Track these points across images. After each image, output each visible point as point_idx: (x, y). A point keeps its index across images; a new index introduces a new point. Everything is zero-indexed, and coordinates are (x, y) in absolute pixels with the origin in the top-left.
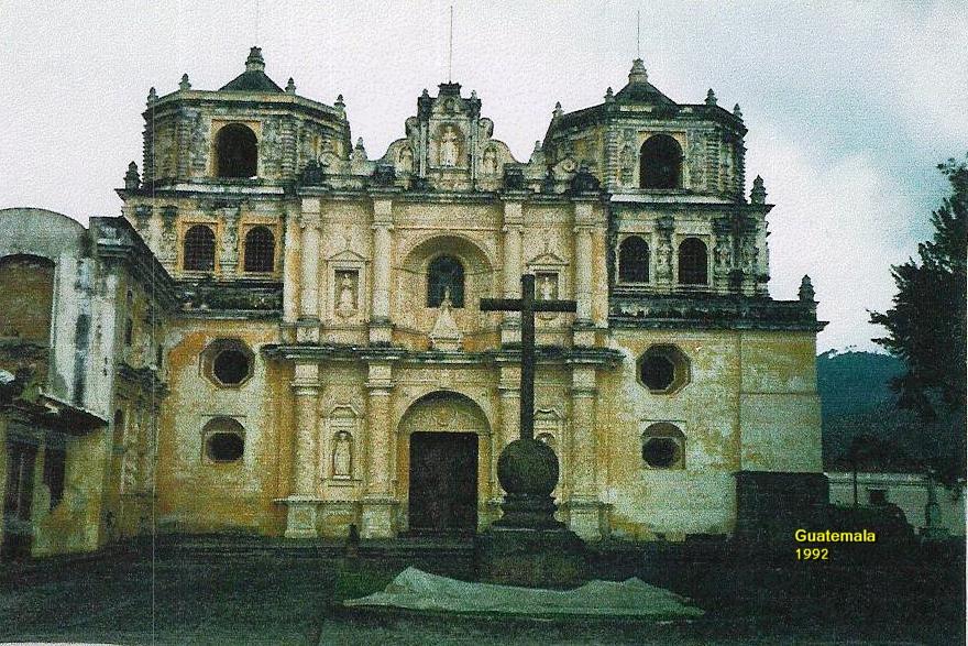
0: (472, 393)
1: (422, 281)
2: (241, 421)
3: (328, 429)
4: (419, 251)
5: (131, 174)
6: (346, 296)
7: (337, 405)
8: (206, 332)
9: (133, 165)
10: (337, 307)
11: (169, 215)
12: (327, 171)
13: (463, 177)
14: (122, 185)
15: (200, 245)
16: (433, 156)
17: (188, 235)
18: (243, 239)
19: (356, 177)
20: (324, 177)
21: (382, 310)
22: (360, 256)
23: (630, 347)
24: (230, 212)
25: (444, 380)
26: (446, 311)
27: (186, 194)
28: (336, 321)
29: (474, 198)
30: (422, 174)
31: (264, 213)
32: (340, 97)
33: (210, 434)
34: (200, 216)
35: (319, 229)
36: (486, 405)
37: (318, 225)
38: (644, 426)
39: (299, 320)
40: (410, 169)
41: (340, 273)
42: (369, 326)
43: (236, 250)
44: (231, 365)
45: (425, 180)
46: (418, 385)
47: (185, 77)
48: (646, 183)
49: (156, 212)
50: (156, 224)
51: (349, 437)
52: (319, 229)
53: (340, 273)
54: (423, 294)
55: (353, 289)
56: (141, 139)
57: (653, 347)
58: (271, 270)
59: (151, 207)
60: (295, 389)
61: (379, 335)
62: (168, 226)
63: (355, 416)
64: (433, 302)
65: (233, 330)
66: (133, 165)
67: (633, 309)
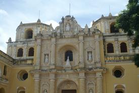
0: (73, 79)
2: (25, 88)
4: (61, 49)
6: (47, 59)
9: (10, 38)
16: (64, 29)
23: (111, 66)
25: (67, 77)
29: (74, 37)
36: (77, 83)
38: (115, 86)
41: (45, 55)
48: (111, 32)
53: (45, 55)
54: (64, 58)
57: (116, 67)
66: (10, 38)
67: (111, 58)
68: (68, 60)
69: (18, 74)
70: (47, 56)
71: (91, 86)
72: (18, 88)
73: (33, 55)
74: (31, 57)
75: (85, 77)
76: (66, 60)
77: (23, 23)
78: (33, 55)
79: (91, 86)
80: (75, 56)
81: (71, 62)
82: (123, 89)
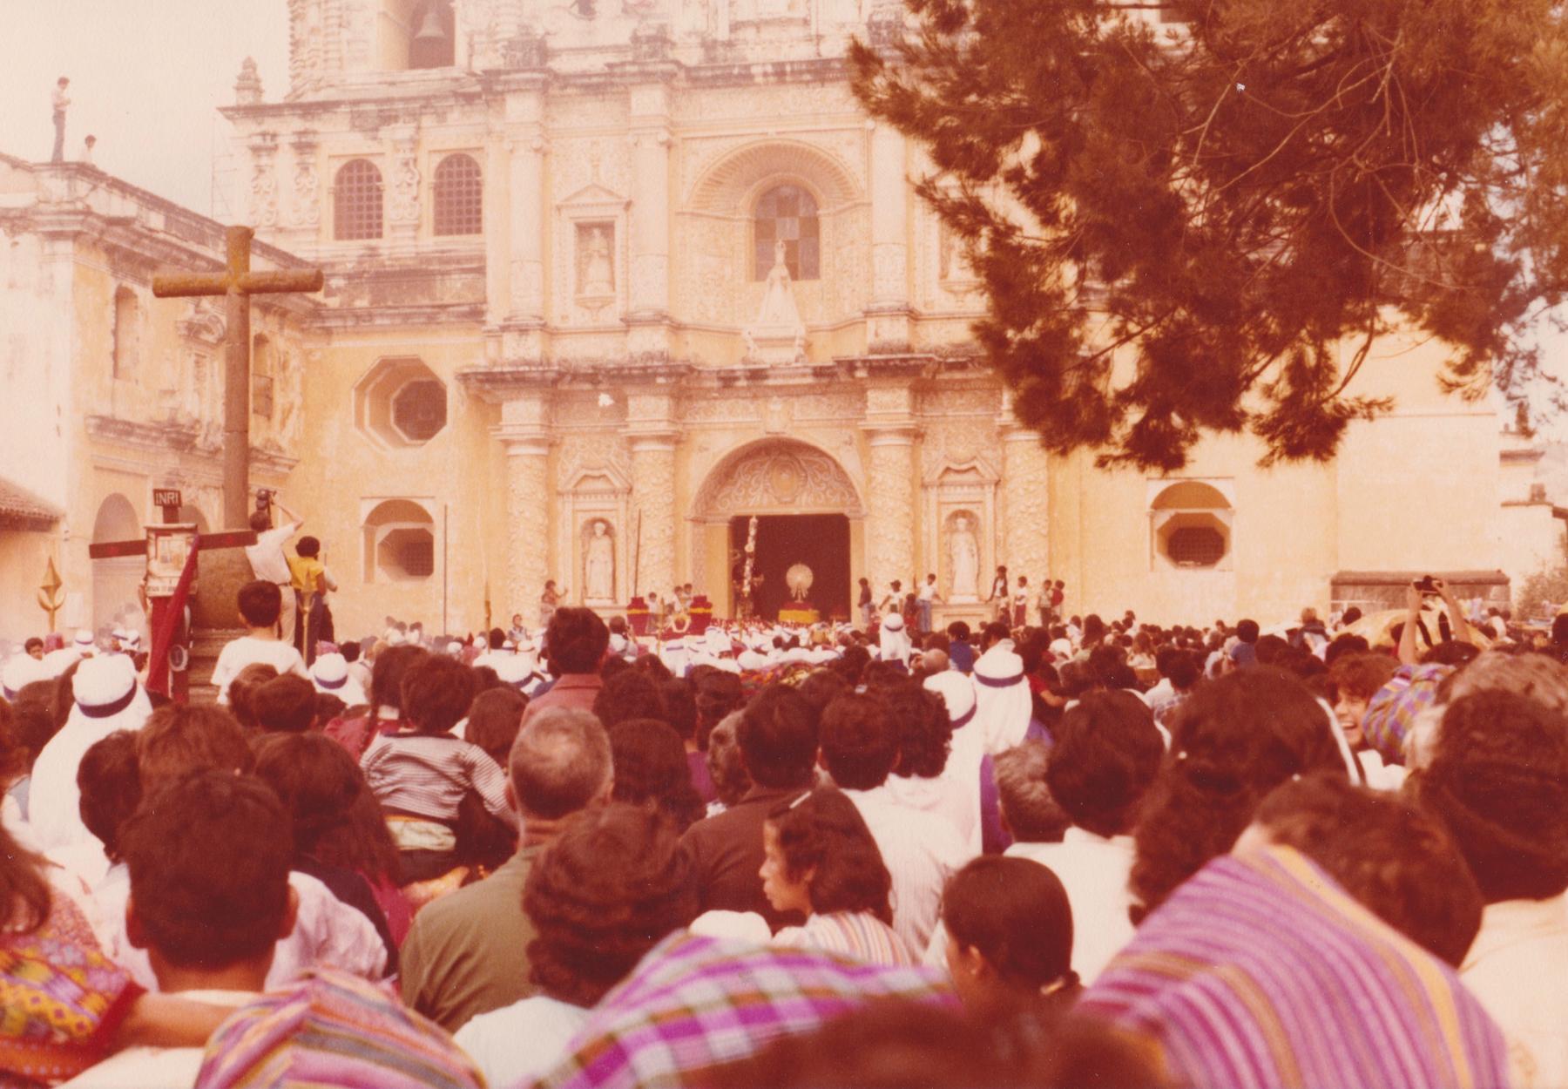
1: (741, 234)
2: (428, 506)
3: (570, 517)
5: (249, 80)
6: (597, 270)
7: (584, 472)
8: (358, 353)
9: (249, 65)
10: (579, 290)
11: (304, 146)
12: (553, 43)
13: (797, 32)
14: (232, 99)
15: (359, 200)
17: (339, 179)
18: (429, 178)
19: (601, 49)
20: (545, 53)
21: (649, 294)
22: (610, 193)
24: (403, 130)
26: (778, 288)
27: (326, 107)
28: (578, 318)
30: (723, 34)
31: (453, 132)
33: (383, 532)
34: (355, 144)
35: (537, 150)
36: (849, 461)
37: (537, 144)
39: (509, 319)
40: (701, 25)
41: (584, 229)
42: (630, 323)
43: (415, 199)
44: (416, 405)
45: (730, 44)
46: (728, 427)
49: (286, 140)
50: (285, 160)
51: (609, 531)
52: (537, 150)
53: (584, 229)
55: (610, 258)
59: (274, 136)
60: (507, 443)
61: (648, 342)
62: (305, 168)
63: (614, 492)
64: (760, 271)
65: (402, 345)
66: (249, 65)
68: (780, 270)
69: (361, 388)
70: (597, 241)
71: (958, 495)
72: (367, 508)
73: (479, 231)
74: (460, 244)
75: (910, 423)
76: (760, 271)
78: (479, 231)
79: (958, 495)
80: (837, 241)
81: (805, 285)
82: (1219, 514)
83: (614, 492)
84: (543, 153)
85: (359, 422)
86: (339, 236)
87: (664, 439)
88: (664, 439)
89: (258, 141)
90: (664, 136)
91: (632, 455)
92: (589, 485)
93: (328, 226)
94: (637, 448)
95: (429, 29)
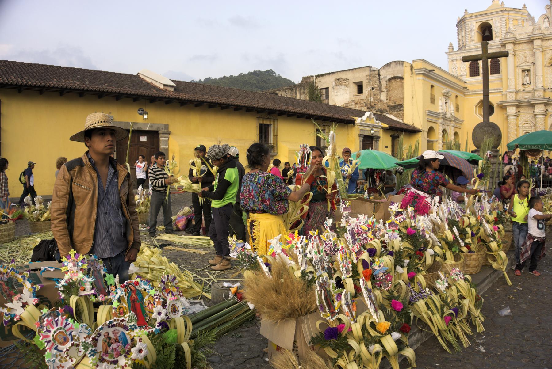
14: (447, 51)
32: (525, 5)
41: (523, 71)
47: (466, 10)
53: (523, 71)
56: (456, 34)
58: (499, 73)
63: (531, 126)
69: (476, 106)
77: (470, 11)
83: (531, 126)
84: (514, 55)
85: (476, 113)
86: (470, 76)
87: (543, 114)
88: (543, 114)
89: (454, 58)
90: (541, 50)
91: (535, 118)
92: (526, 125)
93: (468, 74)
94: (537, 117)
95: (487, 34)
